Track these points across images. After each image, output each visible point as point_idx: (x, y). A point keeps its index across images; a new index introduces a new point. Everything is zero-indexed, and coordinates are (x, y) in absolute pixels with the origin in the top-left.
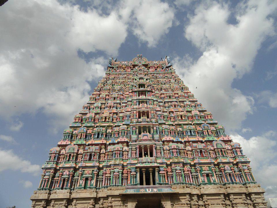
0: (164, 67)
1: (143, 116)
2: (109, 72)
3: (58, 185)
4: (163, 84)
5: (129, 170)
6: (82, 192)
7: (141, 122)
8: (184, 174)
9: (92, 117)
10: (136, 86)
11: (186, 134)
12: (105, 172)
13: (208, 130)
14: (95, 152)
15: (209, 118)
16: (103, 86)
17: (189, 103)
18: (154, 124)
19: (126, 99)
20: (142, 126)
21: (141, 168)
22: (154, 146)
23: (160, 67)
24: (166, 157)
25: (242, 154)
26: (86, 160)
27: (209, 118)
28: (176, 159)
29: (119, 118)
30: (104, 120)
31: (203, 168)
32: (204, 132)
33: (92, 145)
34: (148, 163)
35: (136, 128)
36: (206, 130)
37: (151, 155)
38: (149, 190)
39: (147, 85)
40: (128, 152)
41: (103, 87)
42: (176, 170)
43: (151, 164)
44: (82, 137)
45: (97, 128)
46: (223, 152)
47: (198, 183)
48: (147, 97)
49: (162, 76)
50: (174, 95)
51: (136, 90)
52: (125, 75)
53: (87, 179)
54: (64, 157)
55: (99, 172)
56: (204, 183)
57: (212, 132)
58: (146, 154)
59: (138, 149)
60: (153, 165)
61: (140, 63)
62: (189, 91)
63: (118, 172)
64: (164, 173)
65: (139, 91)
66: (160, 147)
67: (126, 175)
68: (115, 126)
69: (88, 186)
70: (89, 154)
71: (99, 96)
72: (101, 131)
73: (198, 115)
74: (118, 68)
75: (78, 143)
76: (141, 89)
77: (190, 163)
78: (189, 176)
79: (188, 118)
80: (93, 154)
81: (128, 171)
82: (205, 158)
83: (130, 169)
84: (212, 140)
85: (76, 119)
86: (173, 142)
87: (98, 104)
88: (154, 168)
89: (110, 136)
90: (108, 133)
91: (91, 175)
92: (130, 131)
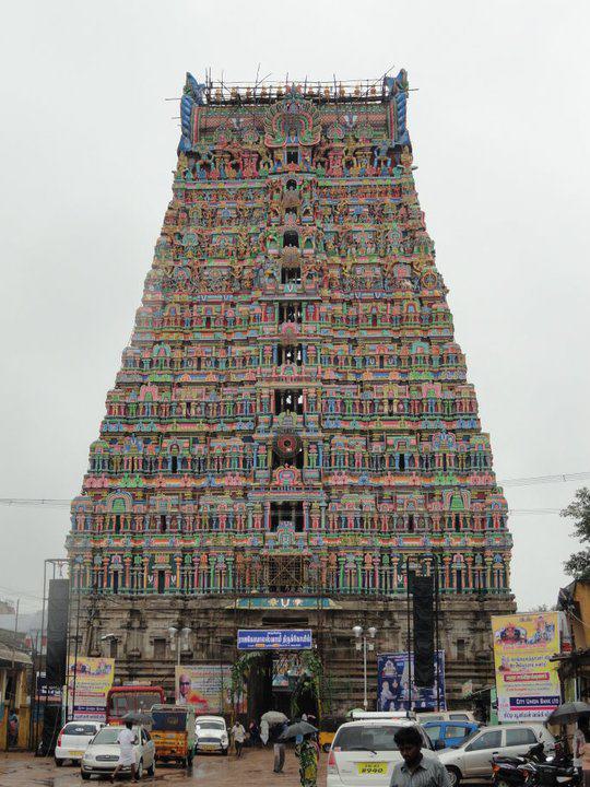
3: (105, 584)
44: (136, 469)
53: (162, 573)
69: (167, 587)
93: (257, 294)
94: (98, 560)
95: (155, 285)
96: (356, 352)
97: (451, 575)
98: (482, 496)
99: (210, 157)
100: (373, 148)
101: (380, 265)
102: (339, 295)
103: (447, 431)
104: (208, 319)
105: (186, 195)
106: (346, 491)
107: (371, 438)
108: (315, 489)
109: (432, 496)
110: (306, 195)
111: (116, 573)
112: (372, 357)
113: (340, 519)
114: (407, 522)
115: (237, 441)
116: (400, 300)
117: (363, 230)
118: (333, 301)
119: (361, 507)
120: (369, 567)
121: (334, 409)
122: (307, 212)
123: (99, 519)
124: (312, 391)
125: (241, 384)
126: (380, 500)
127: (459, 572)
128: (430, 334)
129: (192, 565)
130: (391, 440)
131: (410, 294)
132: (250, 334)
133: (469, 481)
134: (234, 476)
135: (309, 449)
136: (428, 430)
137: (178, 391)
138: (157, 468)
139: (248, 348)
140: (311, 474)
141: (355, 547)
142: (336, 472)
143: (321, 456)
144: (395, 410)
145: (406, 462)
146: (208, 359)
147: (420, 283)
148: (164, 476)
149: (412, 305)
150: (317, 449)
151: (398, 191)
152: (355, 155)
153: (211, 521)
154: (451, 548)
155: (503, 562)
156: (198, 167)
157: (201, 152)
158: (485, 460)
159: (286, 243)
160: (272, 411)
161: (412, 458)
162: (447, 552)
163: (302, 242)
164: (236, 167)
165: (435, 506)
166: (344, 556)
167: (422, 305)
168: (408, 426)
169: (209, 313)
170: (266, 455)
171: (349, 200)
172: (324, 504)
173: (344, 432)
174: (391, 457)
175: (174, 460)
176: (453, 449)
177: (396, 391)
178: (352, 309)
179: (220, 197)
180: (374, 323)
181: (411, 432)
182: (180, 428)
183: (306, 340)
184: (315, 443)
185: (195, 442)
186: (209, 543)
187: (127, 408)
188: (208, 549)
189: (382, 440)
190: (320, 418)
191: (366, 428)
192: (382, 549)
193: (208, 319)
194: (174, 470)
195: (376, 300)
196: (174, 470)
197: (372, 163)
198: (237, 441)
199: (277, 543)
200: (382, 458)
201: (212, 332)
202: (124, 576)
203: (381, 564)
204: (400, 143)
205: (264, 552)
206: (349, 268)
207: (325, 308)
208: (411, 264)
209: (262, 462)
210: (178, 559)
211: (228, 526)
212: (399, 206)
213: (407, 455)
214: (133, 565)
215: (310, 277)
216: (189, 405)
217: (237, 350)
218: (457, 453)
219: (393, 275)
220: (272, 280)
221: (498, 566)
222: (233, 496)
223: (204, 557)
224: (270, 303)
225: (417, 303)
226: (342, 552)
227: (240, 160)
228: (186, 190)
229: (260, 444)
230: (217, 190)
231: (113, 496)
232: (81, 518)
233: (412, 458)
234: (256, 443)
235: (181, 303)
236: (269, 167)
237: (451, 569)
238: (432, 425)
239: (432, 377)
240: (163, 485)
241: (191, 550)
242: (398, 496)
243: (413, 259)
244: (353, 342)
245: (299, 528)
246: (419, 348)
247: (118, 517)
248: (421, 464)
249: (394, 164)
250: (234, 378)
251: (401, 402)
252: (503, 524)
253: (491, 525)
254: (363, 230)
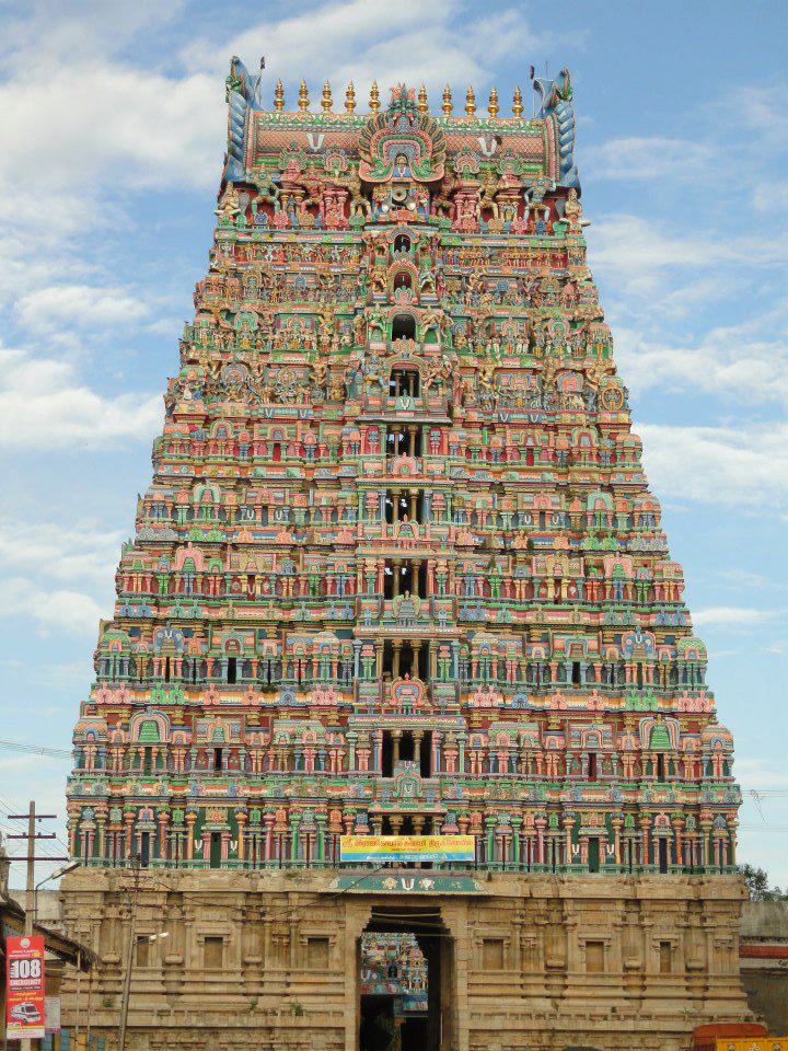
31: (584, 819)
35: (375, 650)
38: (408, 884)
43: (423, 804)
46: (661, 767)
47: (561, 862)
93: (352, 409)
94: (116, 815)
95: (192, 390)
96: (506, 504)
97: (651, 846)
98: (694, 728)
99: (272, 192)
100: (523, 190)
101: (535, 371)
102: (475, 416)
103: (644, 629)
104: (277, 446)
105: (237, 249)
106: (494, 716)
107: (529, 636)
108: (450, 713)
109: (622, 726)
110: (426, 259)
111: (145, 835)
112: (529, 512)
113: (486, 758)
114: (585, 765)
115: (328, 638)
116: (570, 426)
117: (512, 317)
118: (467, 424)
119: (518, 741)
120: (529, 832)
121: (475, 591)
122: (427, 285)
123: (118, 752)
124: (442, 562)
125: (331, 548)
126: (545, 729)
127: (663, 841)
128: (614, 480)
129: (262, 823)
130: (560, 641)
131: (583, 418)
132: (344, 471)
133: (677, 706)
134: (325, 689)
135: (439, 651)
136: (613, 627)
137: (233, 556)
138: (204, 674)
139: (341, 494)
141: (510, 802)
142: (480, 688)
143: (456, 662)
144: (564, 595)
145: (583, 674)
146: (279, 508)
147: (596, 403)
148: (216, 688)
149: (585, 434)
150: (451, 651)
151: (563, 258)
152: (494, 199)
153: (291, 757)
154: (651, 805)
155: (727, 828)
156: (254, 207)
157: (258, 184)
158: (699, 673)
159: (396, 335)
160: (381, 592)
161: (591, 668)
162: (646, 811)
163: (421, 332)
164: (313, 208)
165: (628, 741)
166: (494, 816)
167: (600, 435)
168: (586, 619)
169: (278, 437)
170: (372, 658)
171: (487, 269)
172: (462, 735)
173: (489, 625)
174: (561, 666)
175: (232, 662)
176: (652, 657)
177: (569, 568)
178: (495, 438)
179: (289, 255)
180: (530, 460)
181: (588, 629)
182: (241, 614)
183: (431, 485)
184: (448, 643)
185: (263, 636)
186: (289, 791)
187: (155, 580)
188: (287, 800)
189: (546, 640)
190: (454, 603)
191: (521, 620)
192: (549, 805)
193: (277, 446)
194: (232, 678)
195: (531, 425)
196: (232, 678)
197: (521, 214)
198: (328, 638)
199: (395, 794)
200: (548, 668)
201: (284, 466)
202: (157, 838)
203: (547, 828)
204: (566, 181)
205: (375, 808)
206: (489, 374)
207: (457, 434)
208: (583, 372)
209: (367, 669)
210: (241, 816)
211: (318, 767)
212: (564, 281)
213: (584, 665)
214: (170, 823)
215: (434, 386)
216: (251, 578)
217: (324, 497)
218: (656, 661)
219: (556, 387)
220: (375, 390)
221: (721, 833)
222: (324, 721)
223: (281, 814)
224: (373, 424)
225: (594, 433)
226: (491, 809)
227: (319, 200)
228: (238, 242)
229: (365, 642)
230: (284, 244)
231: (139, 717)
232: (90, 750)
233: (591, 668)
234: (357, 641)
235: (233, 419)
236: (365, 212)
237: (651, 837)
238: (619, 620)
239: (617, 546)
240: (216, 702)
241: (262, 801)
242: (574, 726)
243: (586, 364)
244: (498, 488)
245: (426, 773)
246: (598, 500)
247: (148, 749)
248: (604, 678)
249: (555, 216)
250: (320, 539)
251: (573, 583)
252: (727, 771)
253: (710, 772)
254: (512, 317)
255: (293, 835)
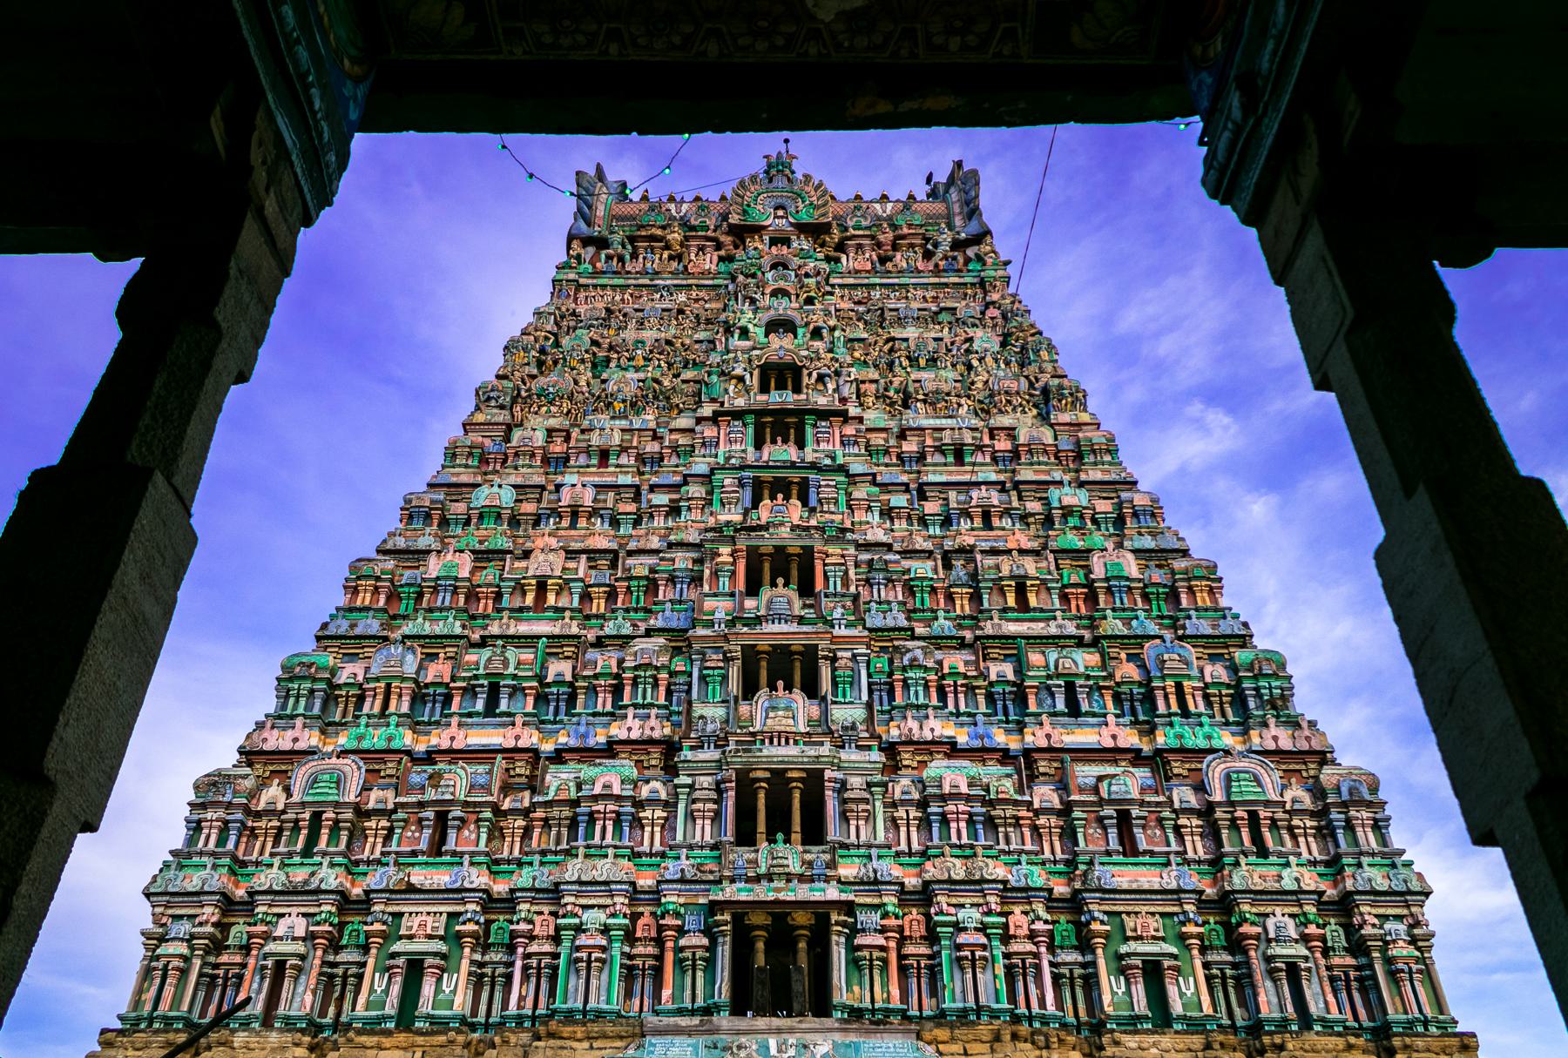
0: (936, 245)
1: (774, 584)
2: (572, 276)
4: (922, 362)
5: (668, 921)
6: (386, 1042)
7: (758, 620)
8: (1007, 956)
9: (456, 579)
10: (741, 379)
11: (1040, 703)
12: (523, 926)
13: (1185, 683)
14: (466, 804)
15: (1203, 599)
16: (535, 371)
17: (1079, 498)
18: (843, 632)
19: (674, 461)
20: (763, 644)
21: (740, 910)
22: (828, 774)
23: (912, 246)
24: (903, 847)
25: (1383, 841)
26: (414, 854)
27: (1203, 599)
28: (958, 862)
29: (628, 588)
30: (530, 599)
32: (1159, 694)
33: (454, 755)
34: (782, 884)
36: (1170, 683)
37: (814, 833)
39: (815, 374)
40: (666, 804)
41: (534, 377)
42: (958, 928)
43: (806, 886)
44: (392, 709)
45: (486, 653)
47: (1090, 1011)
48: (809, 455)
49: (915, 305)
50: (987, 441)
51: (740, 402)
52: (682, 297)
53: (415, 967)
54: (280, 830)
55: (488, 923)
56: (1125, 1018)
57: (1206, 697)
58: (779, 825)
59: (732, 793)
60: (817, 896)
61: (780, 213)
62: (1085, 417)
63: (605, 930)
64: (882, 948)
65: (760, 413)
66: (869, 785)
67: (651, 950)
68: (599, 643)
70: (429, 814)
71: (507, 439)
72: (511, 670)
73: (1127, 579)
74: (634, 248)
75: (365, 745)
76: (776, 398)
77: (1050, 891)
78: (1038, 967)
79: (1064, 598)
80: (457, 812)
81: (660, 929)
82: (1147, 859)
83: (677, 915)
84: (1202, 743)
85: (355, 591)
86: (953, 750)
87: (496, 489)
88: (820, 911)
89: (563, 705)
90: (556, 683)
91: (441, 947)
92: (690, 675)
140: (847, 713)
247: (317, 816)
255: (562, 961)
